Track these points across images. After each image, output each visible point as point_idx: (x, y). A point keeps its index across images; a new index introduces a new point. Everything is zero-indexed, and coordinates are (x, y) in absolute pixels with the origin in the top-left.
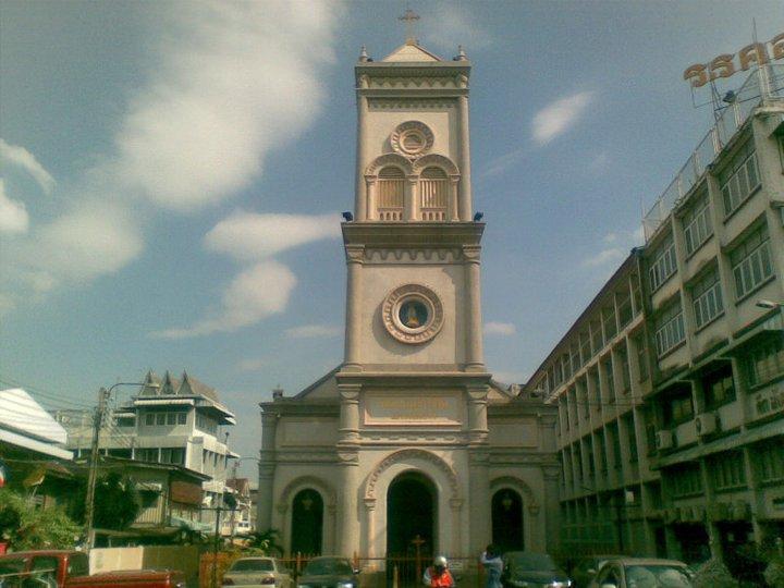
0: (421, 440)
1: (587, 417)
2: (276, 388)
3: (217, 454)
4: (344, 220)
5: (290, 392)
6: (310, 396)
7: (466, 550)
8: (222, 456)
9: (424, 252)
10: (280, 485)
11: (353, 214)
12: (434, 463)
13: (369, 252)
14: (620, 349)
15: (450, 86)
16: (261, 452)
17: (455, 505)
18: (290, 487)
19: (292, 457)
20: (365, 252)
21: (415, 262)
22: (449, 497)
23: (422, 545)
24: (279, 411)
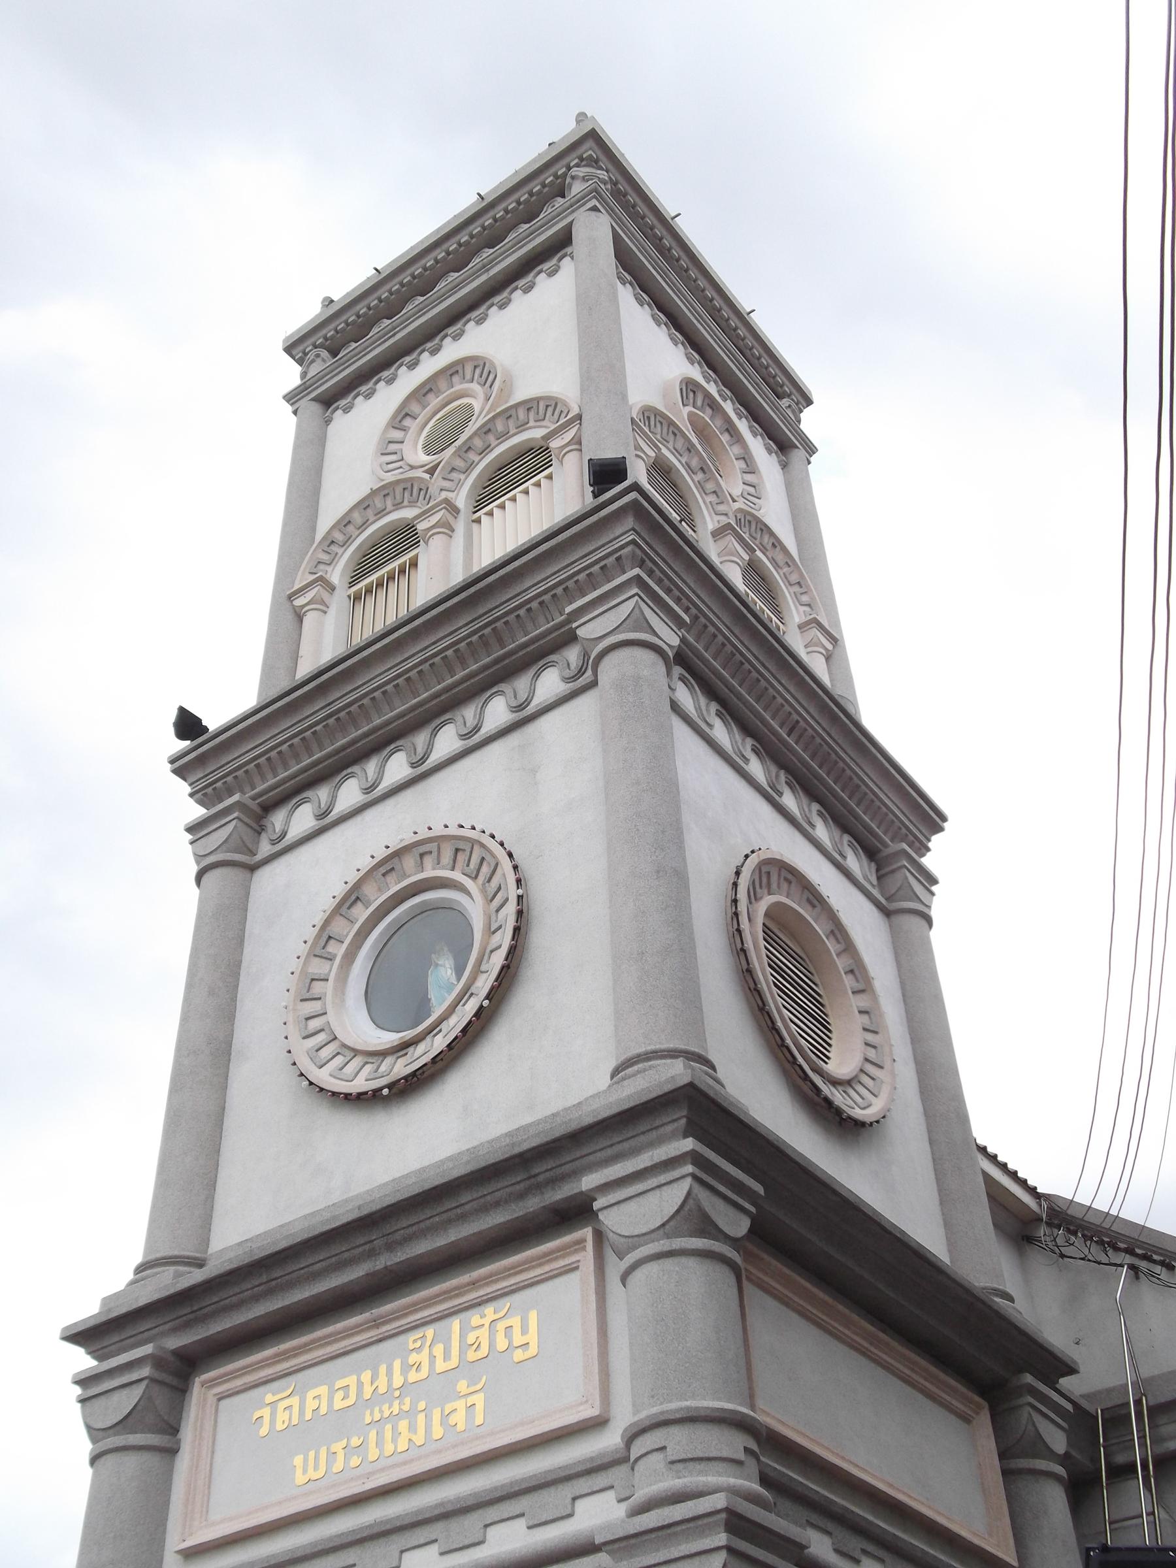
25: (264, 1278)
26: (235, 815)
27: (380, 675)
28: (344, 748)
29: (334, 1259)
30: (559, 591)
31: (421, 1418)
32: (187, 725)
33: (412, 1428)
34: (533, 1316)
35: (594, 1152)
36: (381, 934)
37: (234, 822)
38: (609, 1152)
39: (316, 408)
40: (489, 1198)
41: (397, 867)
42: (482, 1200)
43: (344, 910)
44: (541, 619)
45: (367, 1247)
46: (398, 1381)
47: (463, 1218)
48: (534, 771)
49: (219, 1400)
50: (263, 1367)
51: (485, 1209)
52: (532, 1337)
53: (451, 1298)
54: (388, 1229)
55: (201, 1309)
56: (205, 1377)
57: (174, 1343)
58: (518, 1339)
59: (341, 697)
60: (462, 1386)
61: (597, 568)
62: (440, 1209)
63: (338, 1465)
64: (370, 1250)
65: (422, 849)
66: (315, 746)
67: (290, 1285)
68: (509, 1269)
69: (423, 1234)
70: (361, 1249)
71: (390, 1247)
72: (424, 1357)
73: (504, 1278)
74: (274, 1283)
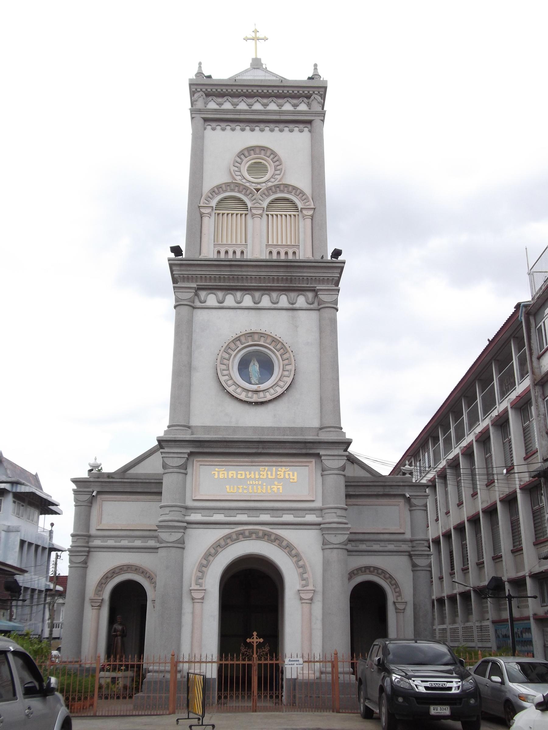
0: (265, 517)
1: (460, 504)
2: (92, 462)
3: (37, 546)
4: (172, 255)
5: (110, 467)
6: (132, 471)
7: (317, 653)
8: (44, 549)
9: (269, 295)
10: (95, 574)
11: (183, 248)
12: (280, 546)
13: (203, 294)
14: (502, 423)
15: (303, 107)
16: (73, 536)
17: (303, 596)
18: (106, 578)
19: (111, 543)
20: (196, 295)
21: (259, 305)
22: (298, 587)
23: (260, 645)
24: (95, 488)
27: (253, 273)
30: (314, 278)
31: (264, 487)
33: (262, 488)
34: (296, 474)
39: (202, 121)
43: (234, 341)
46: (257, 477)
48: (297, 327)
52: (295, 477)
58: (291, 477)
59: (237, 272)
60: (276, 483)
61: (326, 278)
63: (240, 491)
65: (262, 335)
66: (222, 280)
67: (232, 448)
71: (263, 448)
72: (265, 473)
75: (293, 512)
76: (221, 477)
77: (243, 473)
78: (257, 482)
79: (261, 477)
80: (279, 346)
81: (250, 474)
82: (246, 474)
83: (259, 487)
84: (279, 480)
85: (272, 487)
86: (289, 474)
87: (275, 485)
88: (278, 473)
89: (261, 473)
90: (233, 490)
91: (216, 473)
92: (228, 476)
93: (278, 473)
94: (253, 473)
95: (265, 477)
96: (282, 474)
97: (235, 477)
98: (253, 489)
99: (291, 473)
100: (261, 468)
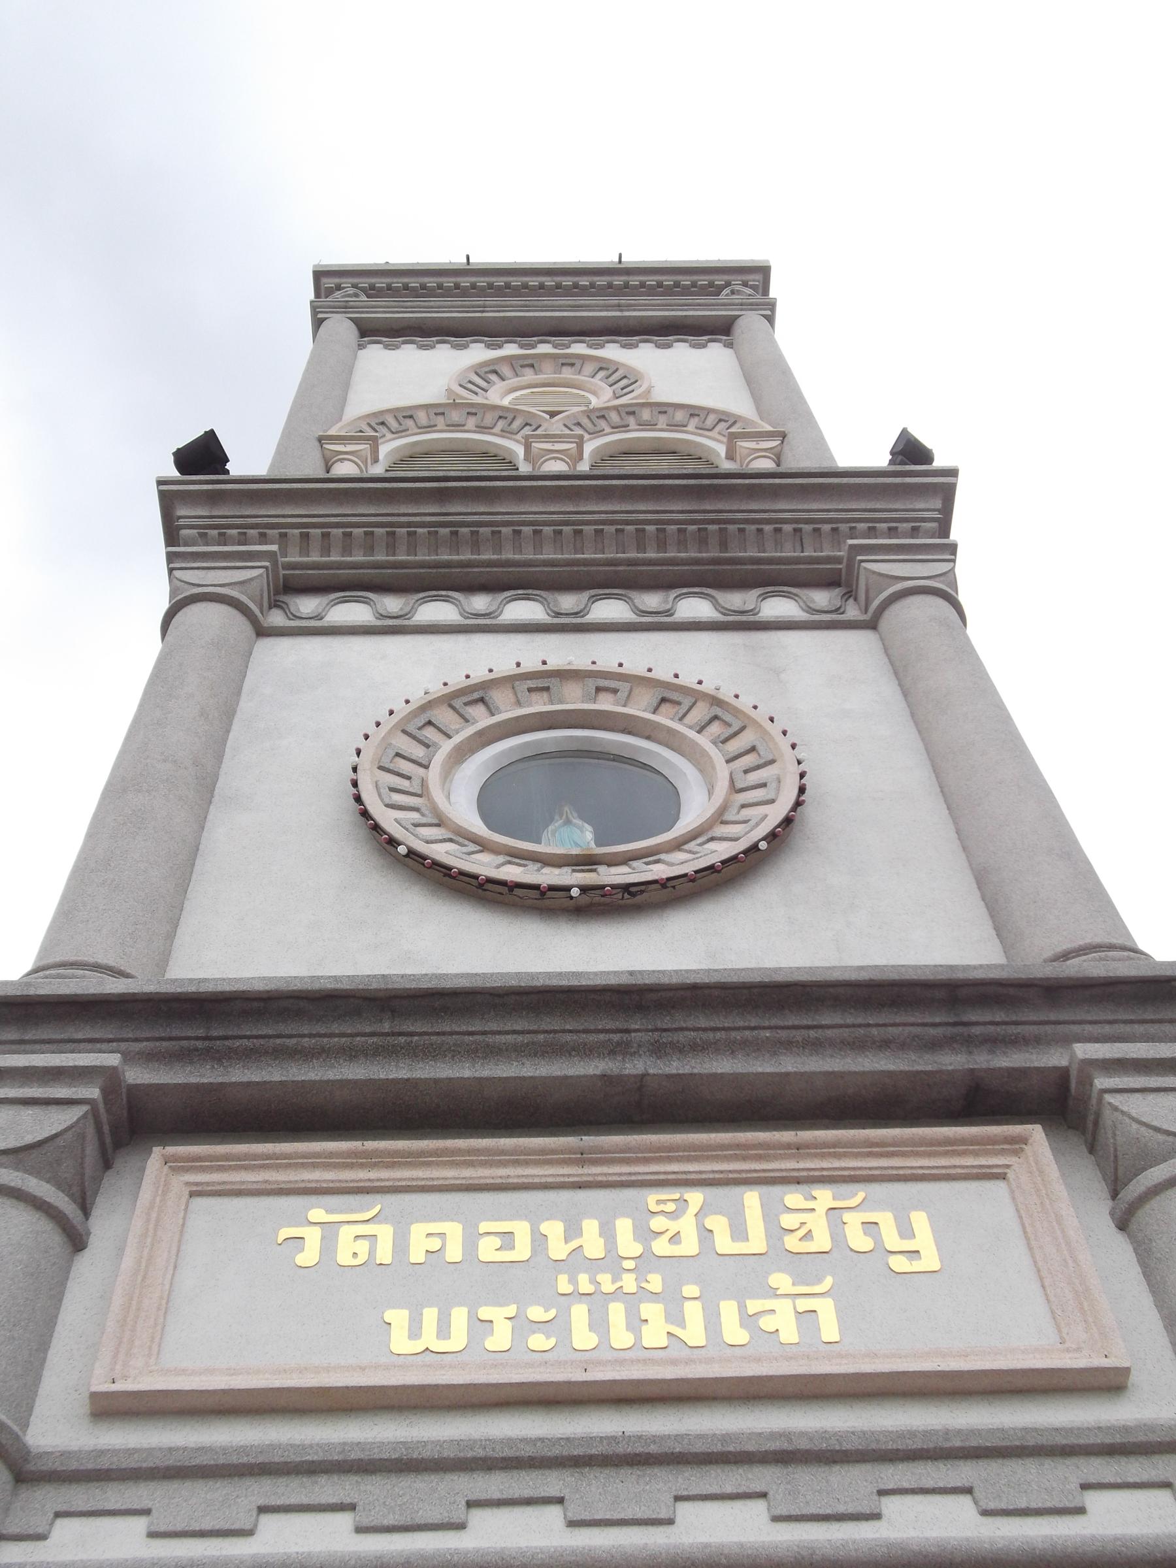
25: (386, 1027)
26: (267, 564)
28: (448, 565)
29: (541, 1037)
32: (203, 456)
33: (676, 1317)
34: (920, 1220)
35: (1080, 1022)
36: (503, 753)
37: (261, 571)
38: (1107, 1029)
40: (874, 1031)
41: (554, 690)
42: (862, 1031)
44: (788, 545)
45: (616, 1037)
47: (816, 1046)
49: (192, 1194)
50: (314, 1166)
51: (859, 1045)
53: (745, 1158)
54: (666, 1022)
55: (226, 1038)
56: (171, 1150)
57: (137, 1076)
58: (892, 1240)
60: (781, 1281)
62: (774, 1022)
64: (618, 1044)
68: (877, 1145)
69: (732, 1048)
70: (602, 1036)
71: (658, 1050)
73: (856, 1156)
74: (402, 1039)
75: (963, 1473)
76: (344, 1258)
77: (521, 1229)
78: (629, 1283)
79: (661, 1247)
80: (700, 713)
81: (572, 1231)
82: (539, 1241)
83: (651, 1310)
84: (805, 1266)
85: (753, 1306)
86: (870, 1227)
87: (774, 1293)
88: (788, 1221)
89: (657, 1223)
90: (443, 1331)
91: (313, 1237)
92: (401, 1245)
93: (788, 1221)
94: (591, 1227)
95: (690, 1245)
96: (819, 1225)
97: (454, 1252)
98: (599, 1324)
99: (886, 1221)
100: (652, 1198)
